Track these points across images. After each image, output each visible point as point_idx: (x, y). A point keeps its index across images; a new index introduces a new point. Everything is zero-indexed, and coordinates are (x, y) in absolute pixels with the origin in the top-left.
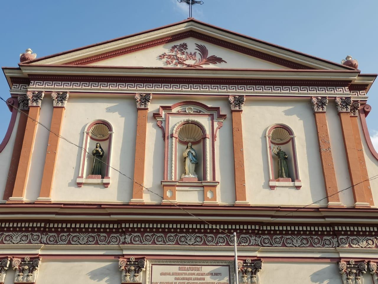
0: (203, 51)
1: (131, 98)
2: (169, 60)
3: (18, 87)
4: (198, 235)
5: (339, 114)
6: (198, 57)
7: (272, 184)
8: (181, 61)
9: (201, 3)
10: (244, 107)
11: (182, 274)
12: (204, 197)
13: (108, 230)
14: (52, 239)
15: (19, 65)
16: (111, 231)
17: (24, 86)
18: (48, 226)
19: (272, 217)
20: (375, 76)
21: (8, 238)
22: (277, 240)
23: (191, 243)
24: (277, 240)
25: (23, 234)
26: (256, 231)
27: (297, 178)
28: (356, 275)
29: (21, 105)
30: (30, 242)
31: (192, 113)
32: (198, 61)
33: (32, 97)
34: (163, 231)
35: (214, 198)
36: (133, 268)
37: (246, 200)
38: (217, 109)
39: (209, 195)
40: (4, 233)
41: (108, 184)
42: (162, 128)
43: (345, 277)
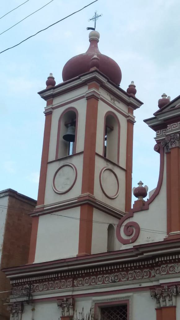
3: (160, 133)
15: (154, 114)
17: (164, 131)
21: (171, 269)
29: (165, 148)
33: (170, 140)
40: (168, 265)
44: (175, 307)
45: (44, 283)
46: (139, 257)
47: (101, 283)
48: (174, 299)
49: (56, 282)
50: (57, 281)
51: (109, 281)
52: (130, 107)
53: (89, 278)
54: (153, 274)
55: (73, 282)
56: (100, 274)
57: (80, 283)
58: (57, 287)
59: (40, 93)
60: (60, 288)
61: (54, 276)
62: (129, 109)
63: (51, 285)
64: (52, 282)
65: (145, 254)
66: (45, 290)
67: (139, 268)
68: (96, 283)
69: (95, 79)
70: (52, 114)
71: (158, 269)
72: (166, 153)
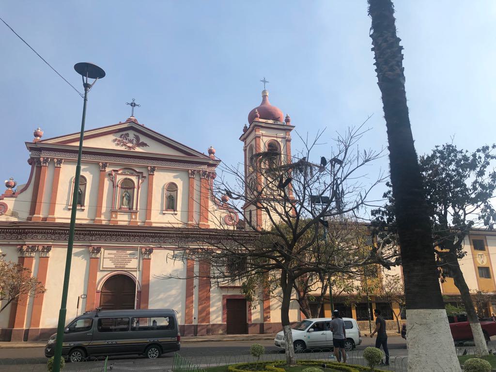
0: (138, 138)
1: (98, 163)
6: (135, 142)
7: (164, 212)
10: (155, 173)
11: (117, 254)
12: (131, 218)
16: (86, 234)
27: (176, 209)
30: (46, 239)
31: (128, 174)
34: (110, 235)
35: (136, 218)
36: (96, 251)
37: (150, 219)
38: (142, 173)
39: (133, 217)
42: (113, 181)
46: (14, 227)
54: (19, 237)
67: (10, 233)
72: (37, 167)
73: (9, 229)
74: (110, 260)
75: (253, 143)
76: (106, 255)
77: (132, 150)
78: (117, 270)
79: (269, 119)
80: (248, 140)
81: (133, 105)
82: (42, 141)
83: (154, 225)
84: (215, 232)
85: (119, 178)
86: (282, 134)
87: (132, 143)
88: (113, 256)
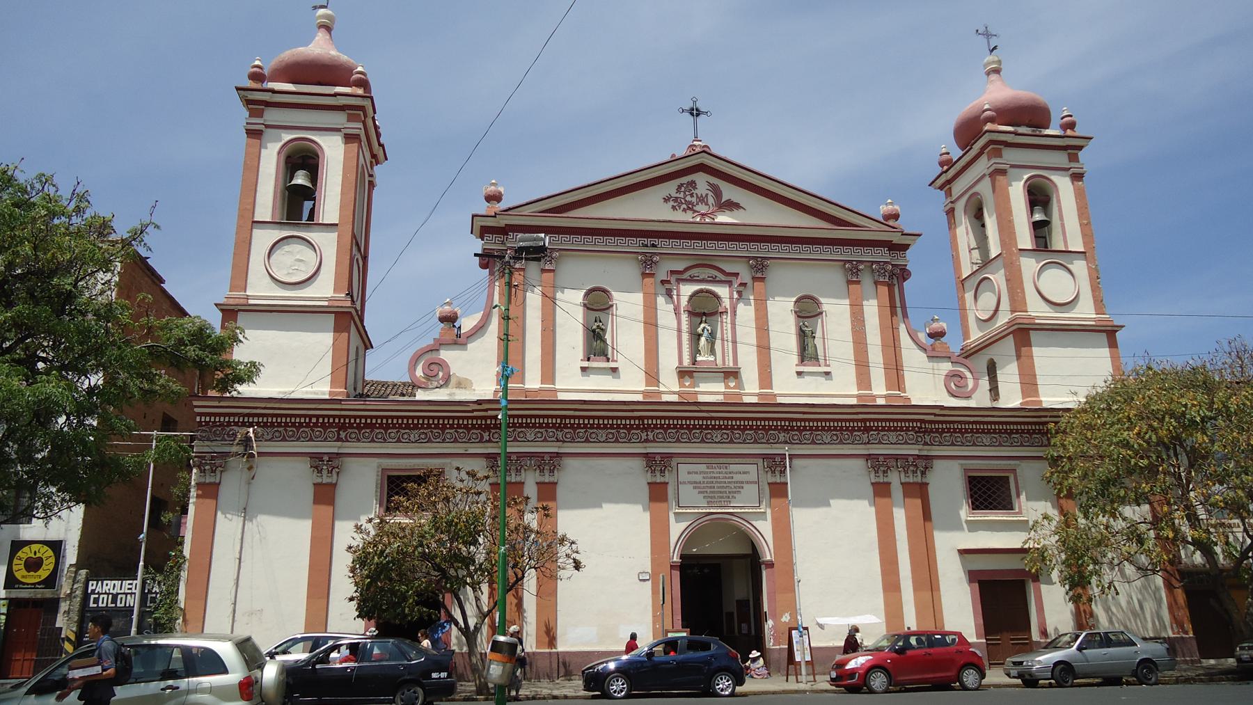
0: (717, 192)
2: (675, 204)
4: (725, 431)
5: (876, 283)
6: (711, 200)
8: (690, 206)
9: (709, 114)
13: (628, 426)
14: (568, 436)
18: (563, 422)
19: (804, 413)
20: (919, 235)
21: (522, 435)
22: (807, 436)
23: (717, 441)
24: (807, 436)
25: (537, 430)
26: (785, 427)
28: (884, 472)
30: (545, 440)
32: (711, 206)
38: (737, 275)
41: (617, 368)
43: (873, 475)
44: (523, 483)
45: (276, 429)
47: (394, 440)
48: (523, 471)
49: (302, 430)
50: (307, 430)
51: (409, 440)
52: (374, 160)
53: (371, 432)
54: (486, 436)
55: (339, 434)
56: (394, 427)
57: (353, 436)
58: (304, 438)
59: (238, 89)
60: (311, 440)
61: (303, 420)
62: (371, 162)
63: (291, 433)
64: (294, 429)
65: (489, 412)
66: (276, 439)
67: (466, 427)
68: (385, 440)
69: (362, 108)
70: (261, 134)
71: (496, 432)
73: (463, 418)
74: (695, 488)
75: (985, 188)
76: (683, 476)
77: (707, 220)
78: (712, 511)
79: (1019, 126)
80: (958, 187)
81: (695, 112)
82: (510, 209)
83: (780, 400)
84: (935, 415)
85: (687, 290)
86: (1060, 159)
87: (707, 204)
88: (699, 478)
